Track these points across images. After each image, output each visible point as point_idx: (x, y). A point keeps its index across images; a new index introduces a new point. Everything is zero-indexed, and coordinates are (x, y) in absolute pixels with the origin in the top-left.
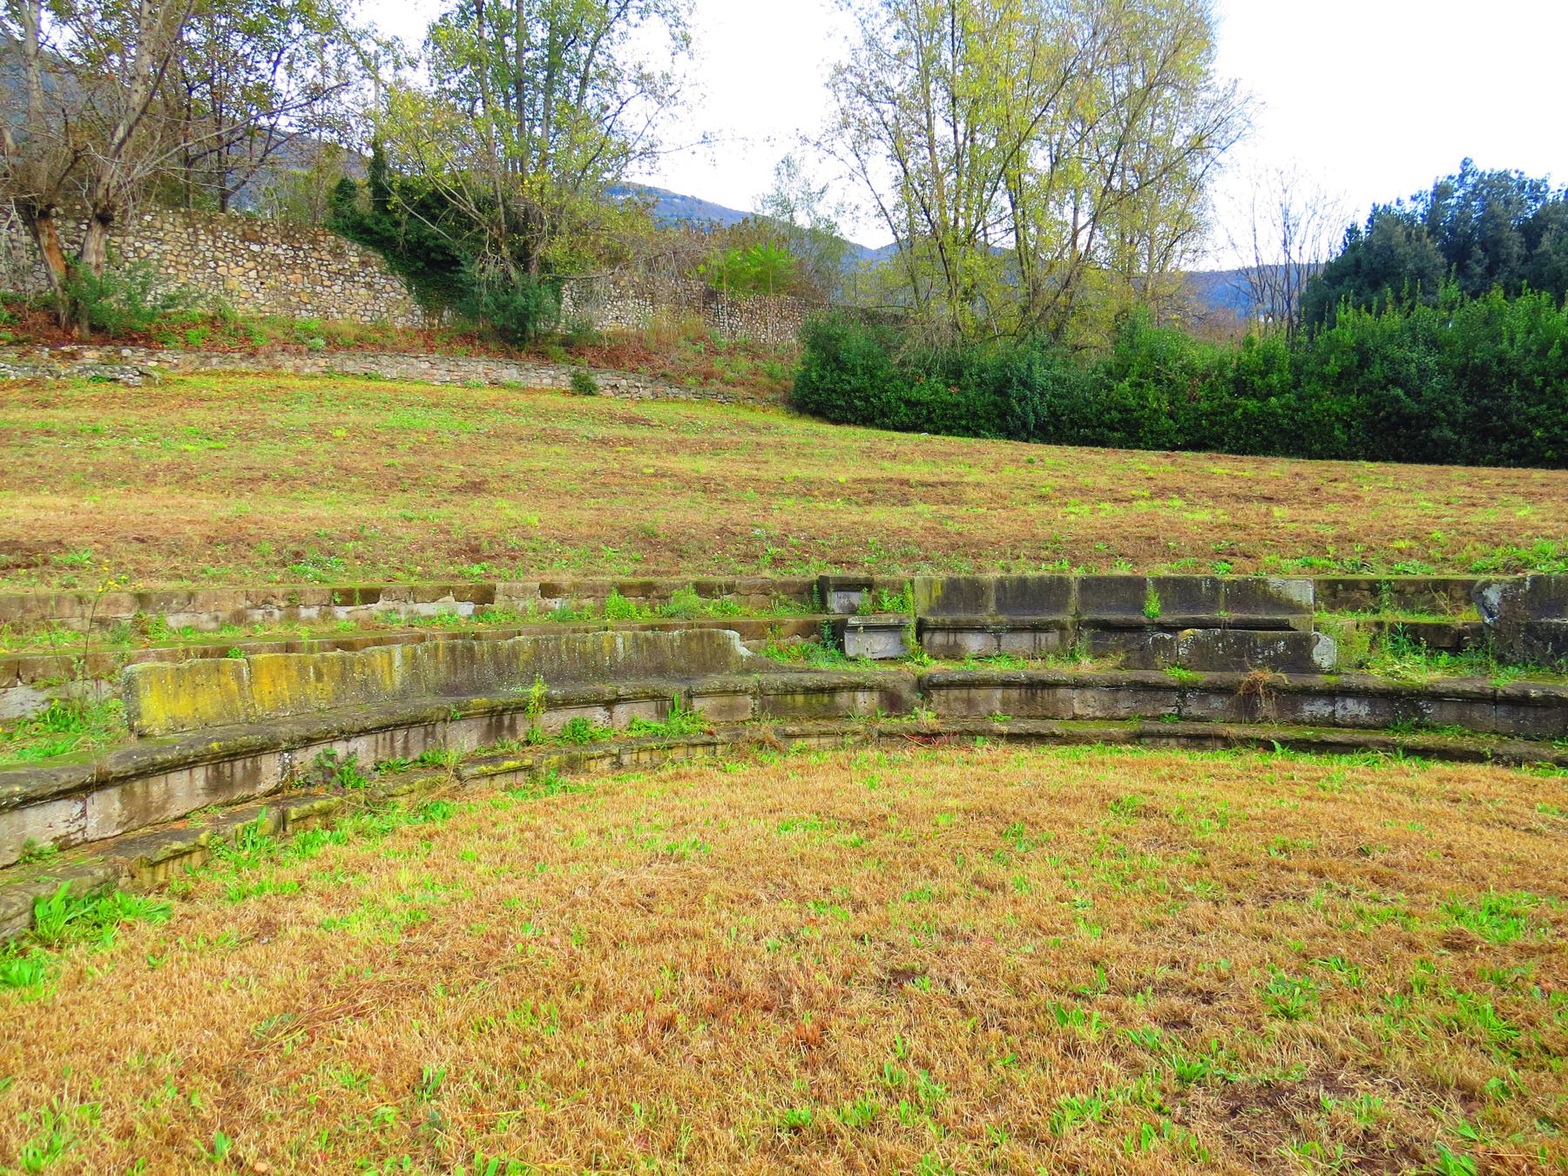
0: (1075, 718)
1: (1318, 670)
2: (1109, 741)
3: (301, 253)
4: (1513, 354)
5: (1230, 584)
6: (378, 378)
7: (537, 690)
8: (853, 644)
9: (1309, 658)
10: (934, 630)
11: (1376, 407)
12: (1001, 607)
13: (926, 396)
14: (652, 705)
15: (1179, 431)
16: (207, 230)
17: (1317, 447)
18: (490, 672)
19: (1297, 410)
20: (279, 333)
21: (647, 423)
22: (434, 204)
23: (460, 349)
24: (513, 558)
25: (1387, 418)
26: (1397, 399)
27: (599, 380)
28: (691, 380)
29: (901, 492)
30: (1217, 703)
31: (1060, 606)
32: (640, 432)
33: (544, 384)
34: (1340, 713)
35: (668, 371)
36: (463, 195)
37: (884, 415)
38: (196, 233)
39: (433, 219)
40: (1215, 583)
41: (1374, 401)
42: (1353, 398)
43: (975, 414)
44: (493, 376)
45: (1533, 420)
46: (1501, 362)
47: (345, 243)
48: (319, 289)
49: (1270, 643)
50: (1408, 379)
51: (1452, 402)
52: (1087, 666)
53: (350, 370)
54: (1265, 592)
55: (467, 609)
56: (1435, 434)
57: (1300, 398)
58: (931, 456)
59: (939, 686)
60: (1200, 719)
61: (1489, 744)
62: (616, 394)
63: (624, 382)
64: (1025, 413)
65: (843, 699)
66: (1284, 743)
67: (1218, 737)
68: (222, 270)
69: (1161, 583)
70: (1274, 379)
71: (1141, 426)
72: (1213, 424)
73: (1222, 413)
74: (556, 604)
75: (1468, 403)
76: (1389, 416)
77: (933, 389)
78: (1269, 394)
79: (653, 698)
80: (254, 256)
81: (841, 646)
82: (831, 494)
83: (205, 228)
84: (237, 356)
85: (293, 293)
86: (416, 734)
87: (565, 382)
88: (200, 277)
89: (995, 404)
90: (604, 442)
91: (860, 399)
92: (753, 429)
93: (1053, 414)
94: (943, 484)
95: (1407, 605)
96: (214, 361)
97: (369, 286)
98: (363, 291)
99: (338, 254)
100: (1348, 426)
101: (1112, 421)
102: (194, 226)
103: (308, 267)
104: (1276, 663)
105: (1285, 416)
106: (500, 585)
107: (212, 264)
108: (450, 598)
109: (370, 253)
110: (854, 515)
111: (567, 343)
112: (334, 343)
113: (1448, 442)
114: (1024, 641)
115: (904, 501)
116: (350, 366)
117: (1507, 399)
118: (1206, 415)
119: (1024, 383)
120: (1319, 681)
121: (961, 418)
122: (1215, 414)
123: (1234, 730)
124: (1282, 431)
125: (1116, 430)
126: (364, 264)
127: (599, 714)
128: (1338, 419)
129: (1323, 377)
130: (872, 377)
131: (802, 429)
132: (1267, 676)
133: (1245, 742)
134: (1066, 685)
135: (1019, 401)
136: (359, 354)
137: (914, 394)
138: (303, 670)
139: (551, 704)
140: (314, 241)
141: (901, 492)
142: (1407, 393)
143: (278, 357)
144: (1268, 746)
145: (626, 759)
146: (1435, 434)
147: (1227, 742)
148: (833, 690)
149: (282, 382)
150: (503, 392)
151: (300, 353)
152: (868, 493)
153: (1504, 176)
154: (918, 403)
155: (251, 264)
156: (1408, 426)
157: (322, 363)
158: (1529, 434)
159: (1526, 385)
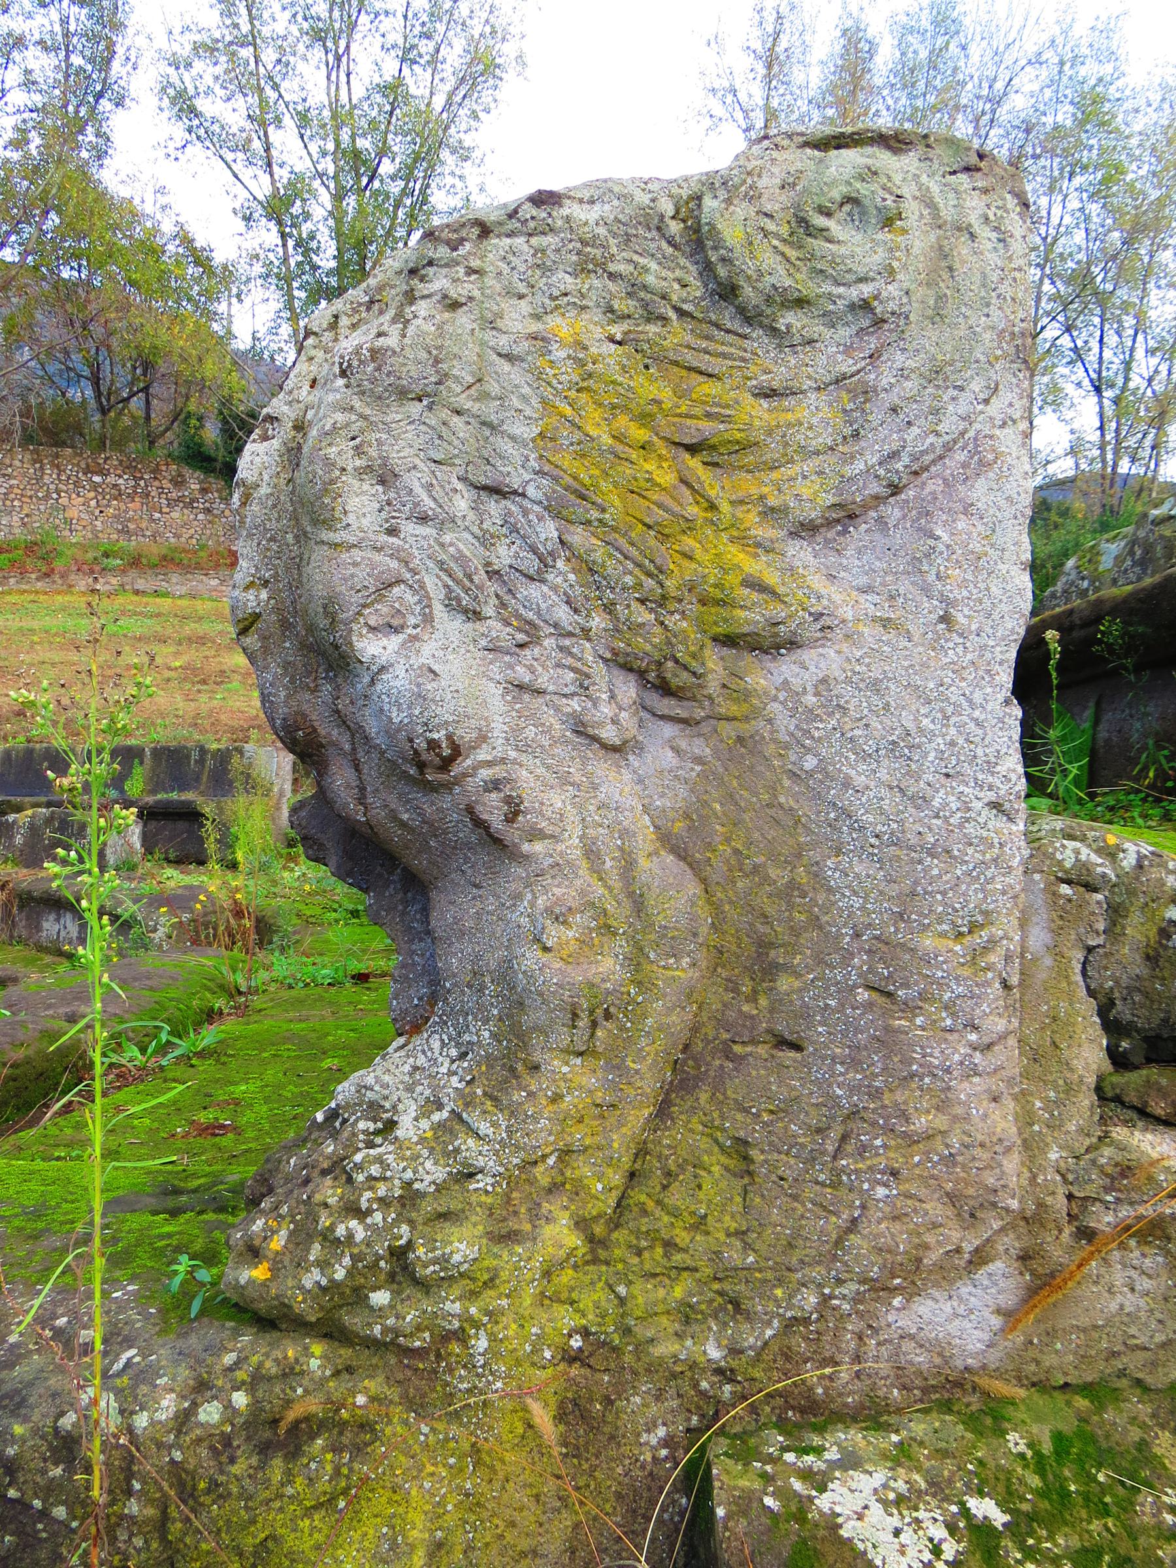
3: (142, 483)
6: (166, 595)
16: (53, 465)
38: (42, 469)
47: (187, 472)
48: (157, 515)
53: (141, 588)
68: (64, 501)
80: (95, 487)
83: (52, 464)
84: (33, 576)
85: (129, 520)
88: (42, 507)
96: (12, 581)
97: (208, 511)
98: (201, 517)
99: (179, 482)
102: (41, 462)
103: (148, 495)
107: (55, 496)
109: (212, 480)
112: (135, 562)
126: (204, 491)
136: (149, 572)
140: (156, 471)
143: (73, 577)
151: (92, 572)
155: (92, 494)
157: (114, 581)
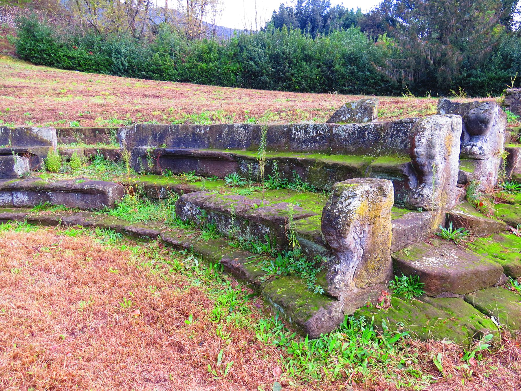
4: (287, 51)
9: (12, 170)
11: (244, 68)
15: (179, 74)
17: (225, 82)
19: (219, 68)
25: (248, 72)
26: (251, 65)
34: (15, 200)
37: (58, 62)
41: (244, 65)
42: (238, 64)
43: (98, 64)
45: (293, 75)
46: (283, 53)
50: (255, 58)
51: (268, 67)
54: (30, 135)
56: (263, 78)
70: (211, 56)
71: (164, 72)
73: (194, 68)
75: (273, 68)
76: (249, 71)
89: (107, 61)
91: (46, 54)
101: (153, 69)
105: (215, 70)
113: (267, 82)
117: (285, 67)
118: (188, 69)
121: (93, 65)
122: (191, 68)
124: (214, 76)
125: (156, 73)
128: (232, 72)
129: (228, 56)
130: (51, 45)
137: (70, 54)
142: (255, 63)
154: (73, 58)
156: (255, 76)
158: (290, 80)
159: (290, 62)
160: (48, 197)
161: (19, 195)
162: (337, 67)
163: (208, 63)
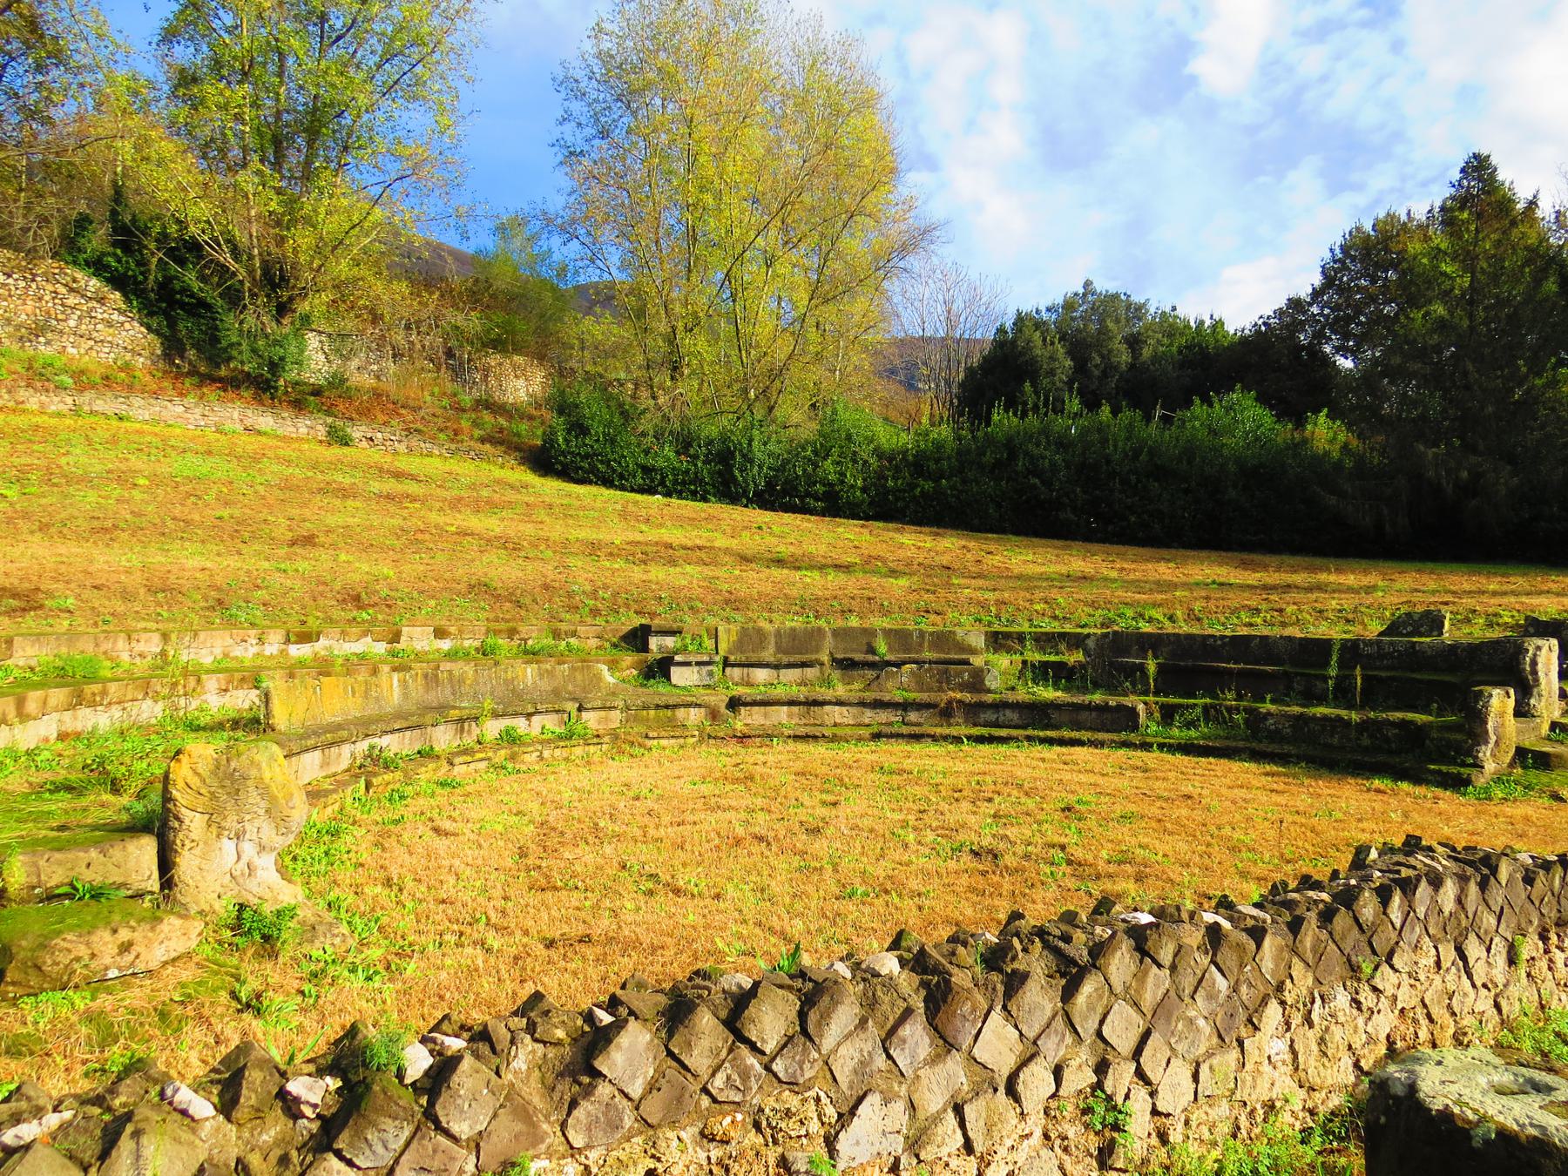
0: (835, 725)
1: (989, 691)
2: (860, 739)
3: (34, 285)
5: (932, 634)
7: (488, 704)
8: (675, 672)
10: (733, 666)
12: (779, 649)
13: (661, 463)
14: (555, 716)
18: (448, 691)
19: (961, 492)
20: (18, 368)
21: (414, 478)
22: (188, 250)
23: (211, 392)
24: (389, 606)
26: (1034, 487)
27: (356, 432)
28: (442, 436)
29: (668, 554)
30: (926, 713)
31: (817, 650)
32: (413, 488)
33: (301, 431)
34: (1002, 718)
35: (419, 426)
36: (219, 245)
37: (621, 477)
39: (181, 262)
40: (922, 634)
44: (248, 422)
49: (959, 674)
52: (840, 690)
55: (381, 648)
56: (1062, 516)
57: (964, 482)
58: (680, 521)
59: (746, 704)
60: (919, 725)
61: (1085, 735)
62: (371, 446)
63: (379, 435)
64: (745, 481)
65: (680, 713)
66: (969, 738)
67: (929, 736)
69: (888, 633)
72: (897, 499)
74: (446, 645)
77: (667, 456)
78: (941, 477)
79: (557, 711)
81: (668, 677)
82: (611, 554)
86: (417, 732)
87: (321, 432)
90: (389, 497)
91: (602, 462)
92: (512, 487)
93: (768, 484)
94: (700, 548)
95: (1042, 650)
100: (999, 506)
104: (963, 687)
106: (405, 630)
108: (369, 639)
110: (637, 573)
111: (317, 392)
112: (82, 381)
114: (794, 674)
115: (672, 562)
116: (99, 405)
119: (744, 456)
120: (989, 698)
123: (939, 730)
127: (520, 724)
131: (551, 488)
132: (959, 696)
133: (945, 738)
134: (830, 703)
135: (741, 471)
138: (345, 689)
139: (496, 715)
141: (668, 554)
142: (1043, 482)
144: (957, 740)
145: (546, 754)
146: (1062, 516)
147: (934, 738)
148: (675, 706)
149: (39, 420)
150: (264, 439)
152: (645, 555)
153: (1116, 296)
154: (653, 469)
157: (69, 400)
160: (1048, 717)
161: (1008, 713)
162: (1232, 493)
163: (937, 480)
